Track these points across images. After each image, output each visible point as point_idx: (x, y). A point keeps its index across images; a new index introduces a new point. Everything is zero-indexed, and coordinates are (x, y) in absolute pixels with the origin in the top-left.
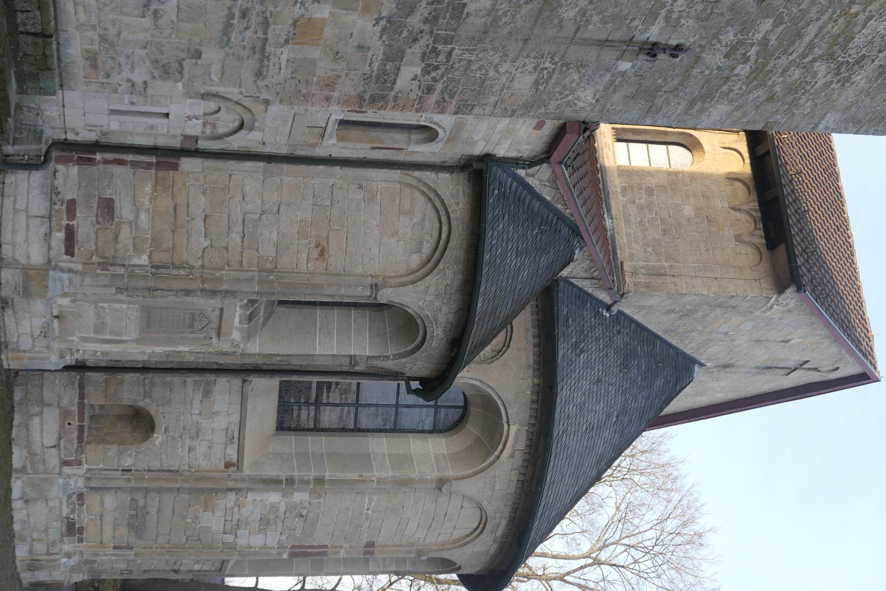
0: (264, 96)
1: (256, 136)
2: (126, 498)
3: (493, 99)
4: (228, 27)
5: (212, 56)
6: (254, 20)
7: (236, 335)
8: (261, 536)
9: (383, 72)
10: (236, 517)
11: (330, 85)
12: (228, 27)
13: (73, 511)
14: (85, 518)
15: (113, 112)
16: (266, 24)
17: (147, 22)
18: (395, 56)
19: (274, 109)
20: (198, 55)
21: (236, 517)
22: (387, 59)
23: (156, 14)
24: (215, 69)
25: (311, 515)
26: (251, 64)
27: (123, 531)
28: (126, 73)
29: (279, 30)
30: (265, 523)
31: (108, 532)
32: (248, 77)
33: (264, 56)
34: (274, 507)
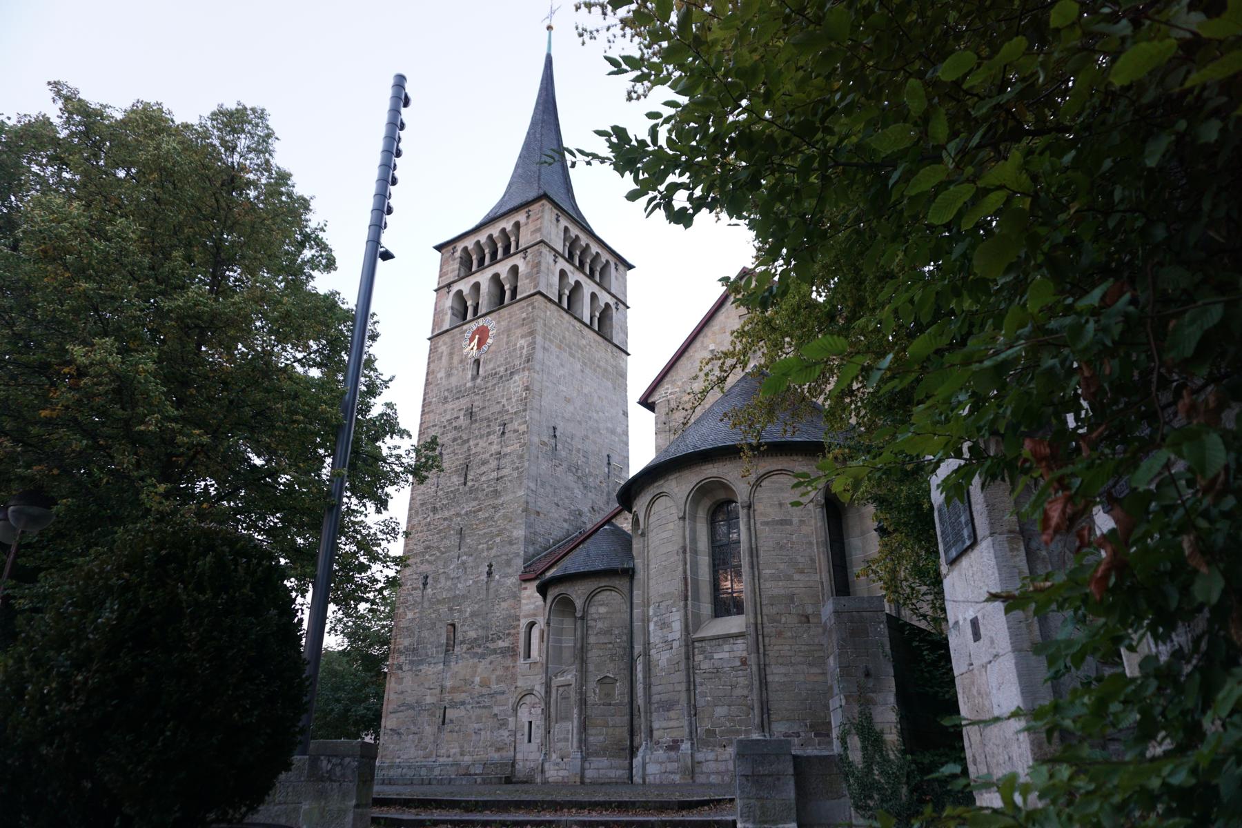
0: (513, 689)
1: (537, 687)
2: (655, 715)
3: (513, 611)
4: (485, 707)
5: (496, 710)
6: (481, 699)
7: (569, 677)
8: (673, 624)
9: (502, 652)
10: (661, 645)
11: (507, 668)
12: (485, 707)
13: (661, 747)
14: (667, 739)
15: (530, 741)
16: (482, 696)
17: (483, 733)
18: (494, 651)
19: (519, 684)
20: (496, 715)
21: (661, 645)
22: (496, 653)
23: (480, 730)
24: (501, 708)
25: (659, 600)
26: (499, 697)
27: (672, 714)
28: (505, 738)
29: (485, 691)
30: (665, 625)
31: (672, 724)
32: (504, 697)
33: (496, 693)
34: (656, 623)
